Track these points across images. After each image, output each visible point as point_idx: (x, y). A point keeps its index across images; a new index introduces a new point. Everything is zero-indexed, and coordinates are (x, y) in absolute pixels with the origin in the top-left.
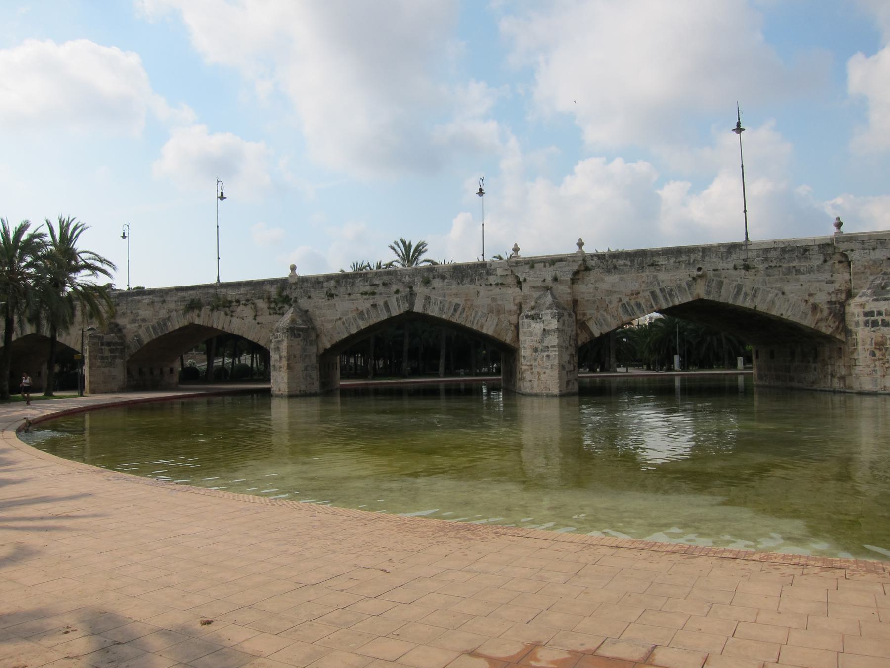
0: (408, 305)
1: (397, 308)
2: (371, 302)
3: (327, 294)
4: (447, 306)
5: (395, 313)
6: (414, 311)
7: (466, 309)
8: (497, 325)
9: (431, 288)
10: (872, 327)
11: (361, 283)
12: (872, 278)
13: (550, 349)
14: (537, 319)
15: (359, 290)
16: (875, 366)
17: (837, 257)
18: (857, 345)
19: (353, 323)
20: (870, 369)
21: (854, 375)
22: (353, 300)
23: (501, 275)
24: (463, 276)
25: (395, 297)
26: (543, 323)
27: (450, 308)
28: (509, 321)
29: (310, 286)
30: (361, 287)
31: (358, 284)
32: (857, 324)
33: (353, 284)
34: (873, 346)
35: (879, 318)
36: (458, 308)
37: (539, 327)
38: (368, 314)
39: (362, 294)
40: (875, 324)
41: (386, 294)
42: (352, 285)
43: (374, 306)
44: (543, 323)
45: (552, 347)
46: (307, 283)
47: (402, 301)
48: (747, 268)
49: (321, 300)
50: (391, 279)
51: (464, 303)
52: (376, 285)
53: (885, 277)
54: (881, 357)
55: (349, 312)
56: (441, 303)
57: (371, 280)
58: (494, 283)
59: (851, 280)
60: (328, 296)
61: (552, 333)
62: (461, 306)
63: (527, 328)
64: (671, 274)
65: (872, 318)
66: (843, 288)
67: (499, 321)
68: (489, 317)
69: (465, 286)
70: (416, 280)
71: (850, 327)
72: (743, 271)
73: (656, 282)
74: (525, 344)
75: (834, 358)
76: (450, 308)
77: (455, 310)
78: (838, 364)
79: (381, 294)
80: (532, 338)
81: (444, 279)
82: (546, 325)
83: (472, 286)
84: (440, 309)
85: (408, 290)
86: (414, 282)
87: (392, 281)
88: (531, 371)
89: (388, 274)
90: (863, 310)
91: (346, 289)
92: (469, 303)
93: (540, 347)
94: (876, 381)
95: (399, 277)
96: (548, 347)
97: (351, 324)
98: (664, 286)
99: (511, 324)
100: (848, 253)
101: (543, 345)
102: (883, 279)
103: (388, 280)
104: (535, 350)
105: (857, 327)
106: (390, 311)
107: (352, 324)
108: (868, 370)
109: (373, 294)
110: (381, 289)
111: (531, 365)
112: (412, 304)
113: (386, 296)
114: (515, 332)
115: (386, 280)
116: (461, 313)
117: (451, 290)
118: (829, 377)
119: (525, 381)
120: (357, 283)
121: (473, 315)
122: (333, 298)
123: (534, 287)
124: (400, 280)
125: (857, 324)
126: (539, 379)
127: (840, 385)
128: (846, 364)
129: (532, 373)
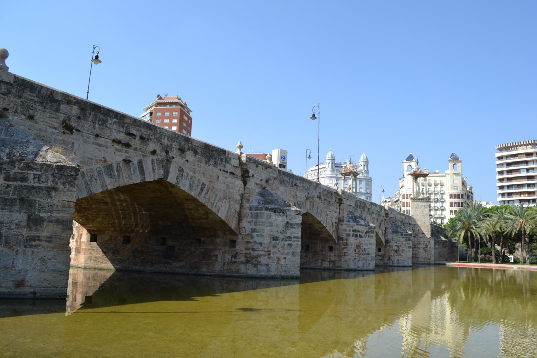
0: (162, 172)
1: (152, 172)
2: (124, 156)
3: (63, 123)
4: (195, 184)
5: (149, 178)
6: (168, 180)
7: (210, 190)
8: (228, 211)
9: (185, 159)
10: (356, 237)
11: (115, 126)
12: (347, 213)
13: (293, 239)
14: (279, 213)
15: (111, 135)
16: (356, 256)
17: (337, 200)
18: (347, 246)
19: (98, 179)
20: (353, 258)
21: (343, 260)
22: (100, 145)
23: (233, 166)
24: (210, 157)
25: (151, 158)
26: (287, 217)
27: (198, 186)
28: (235, 209)
29: (37, 100)
30: (114, 131)
31: (111, 126)
32: (348, 235)
33: (104, 123)
34: (356, 247)
35: (358, 233)
36: (204, 187)
37: (282, 220)
38: (118, 171)
39: (114, 141)
40: (356, 236)
41: (142, 152)
42: (103, 124)
43: (127, 162)
44: (287, 217)
45: (294, 237)
46: (31, 92)
47: (157, 165)
48: (320, 198)
49: (51, 130)
50: (149, 135)
51: (208, 184)
52: (132, 135)
53: (352, 214)
54: (358, 252)
55: (94, 161)
56: (191, 178)
57: (127, 126)
58: (229, 171)
59: (340, 212)
60: (63, 127)
61: (296, 227)
62: (206, 186)
63: (267, 219)
64: (301, 194)
65: (356, 233)
66: (338, 216)
67: (229, 207)
68: (224, 202)
69: (210, 167)
70: (173, 146)
71: (341, 236)
72: (319, 199)
73: (296, 197)
74: (263, 232)
75: (326, 251)
76: (198, 186)
77: (202, 190)
78: (329, 254)
79: (136, 149)
80: (272, 228)
81: (196, 154)
82: (289, 220)
83: (215, 169)
84: (190, 183)
85: (164, 154)
86: (171, 147)
87: (151, 137)
88: (269, 256)
89: (147, 128)
90: (352, 229)
91: (94, 126)
92: (212, 185)
93: (282, 236)
94: (356, 263)
95: (158, 136)
96: (290, 237)
97: (93, 179)
98: (298, 201)
99: (236, 211)
100: (343, 199)
101: (285, 235)
102: (352, 215)
103: (146, 135)
104: (276, 239)
105: (348, 236)
106: (144, 175)
107: (96, 179)
108: (352, 258)
109: (128, 145)
110: (136, 143)
111: (269, 251)
112: (167, 172)
113: (141, 153)
114: (238, 219)
115: (144, 134)
116: (205, 194)
117: (200, 167)
118: (320, 261)
119: (261, 265)
120: (111, 124)
121: (213, 198)
122: (72, 133)
123: (257, 184)
124: (158, 140)
125: (348, 235)
126: (278, 263)
127: (330, 265)
128: (336, 254)
129: (269, 258)
